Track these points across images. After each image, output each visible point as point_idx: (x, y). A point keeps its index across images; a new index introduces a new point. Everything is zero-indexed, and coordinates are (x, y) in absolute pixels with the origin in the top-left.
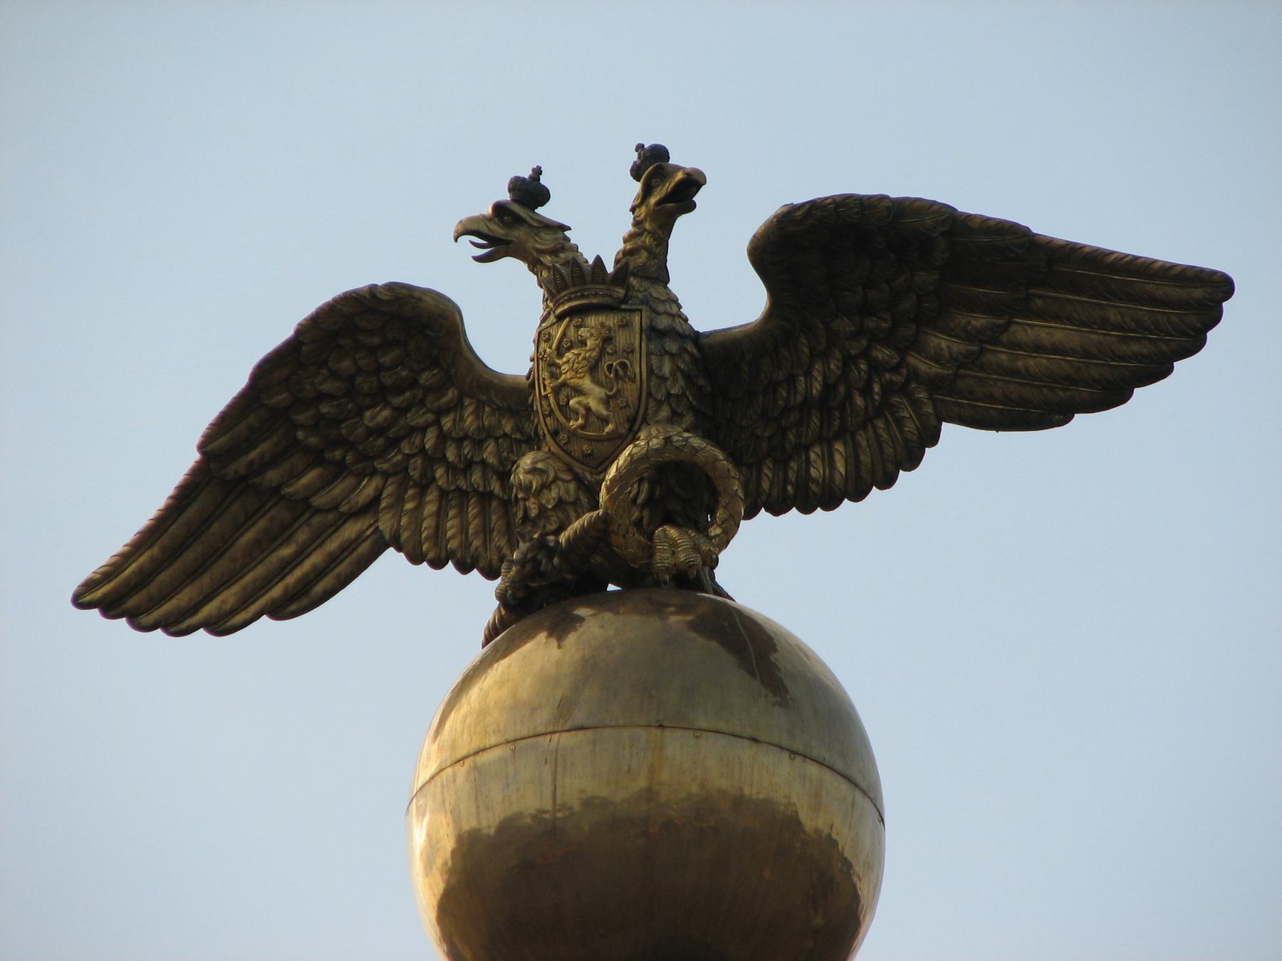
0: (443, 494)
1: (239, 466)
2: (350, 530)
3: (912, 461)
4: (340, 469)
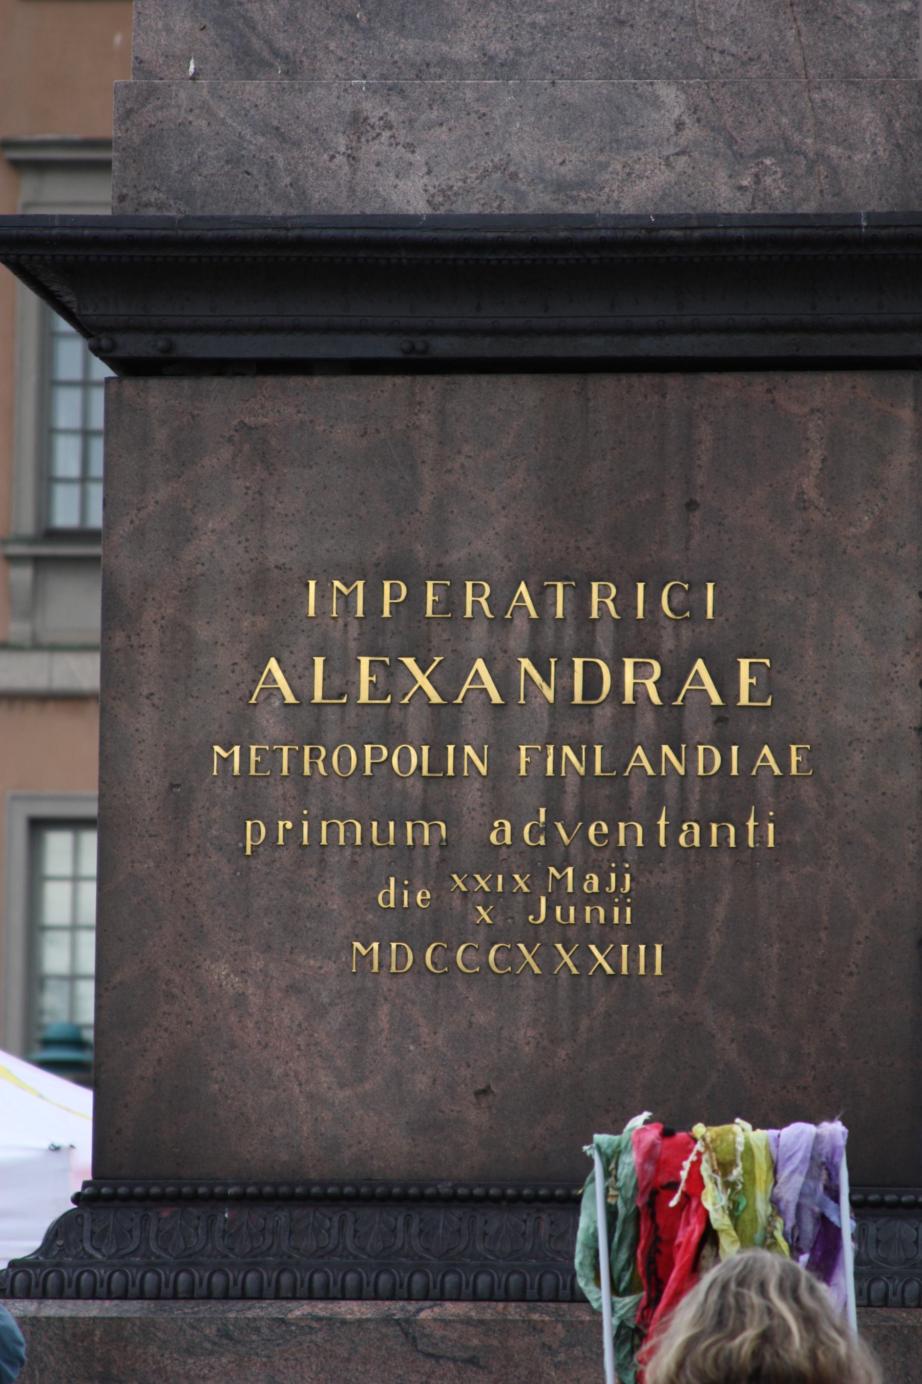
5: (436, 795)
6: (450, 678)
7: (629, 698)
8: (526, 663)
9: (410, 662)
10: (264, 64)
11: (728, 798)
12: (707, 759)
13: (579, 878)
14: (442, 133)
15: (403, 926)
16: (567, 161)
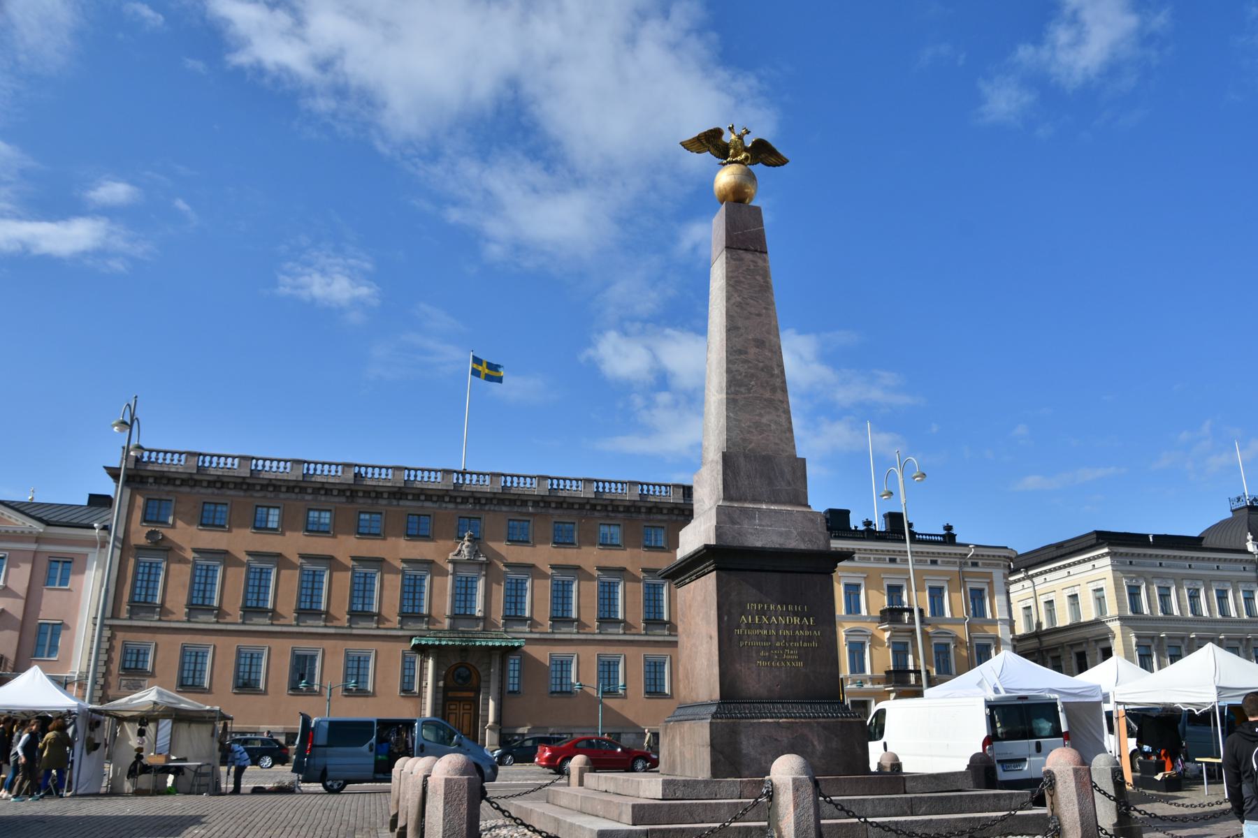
5: (769, 637)
6: (769, 619)
11: (809, 639)
12: (807, 633)
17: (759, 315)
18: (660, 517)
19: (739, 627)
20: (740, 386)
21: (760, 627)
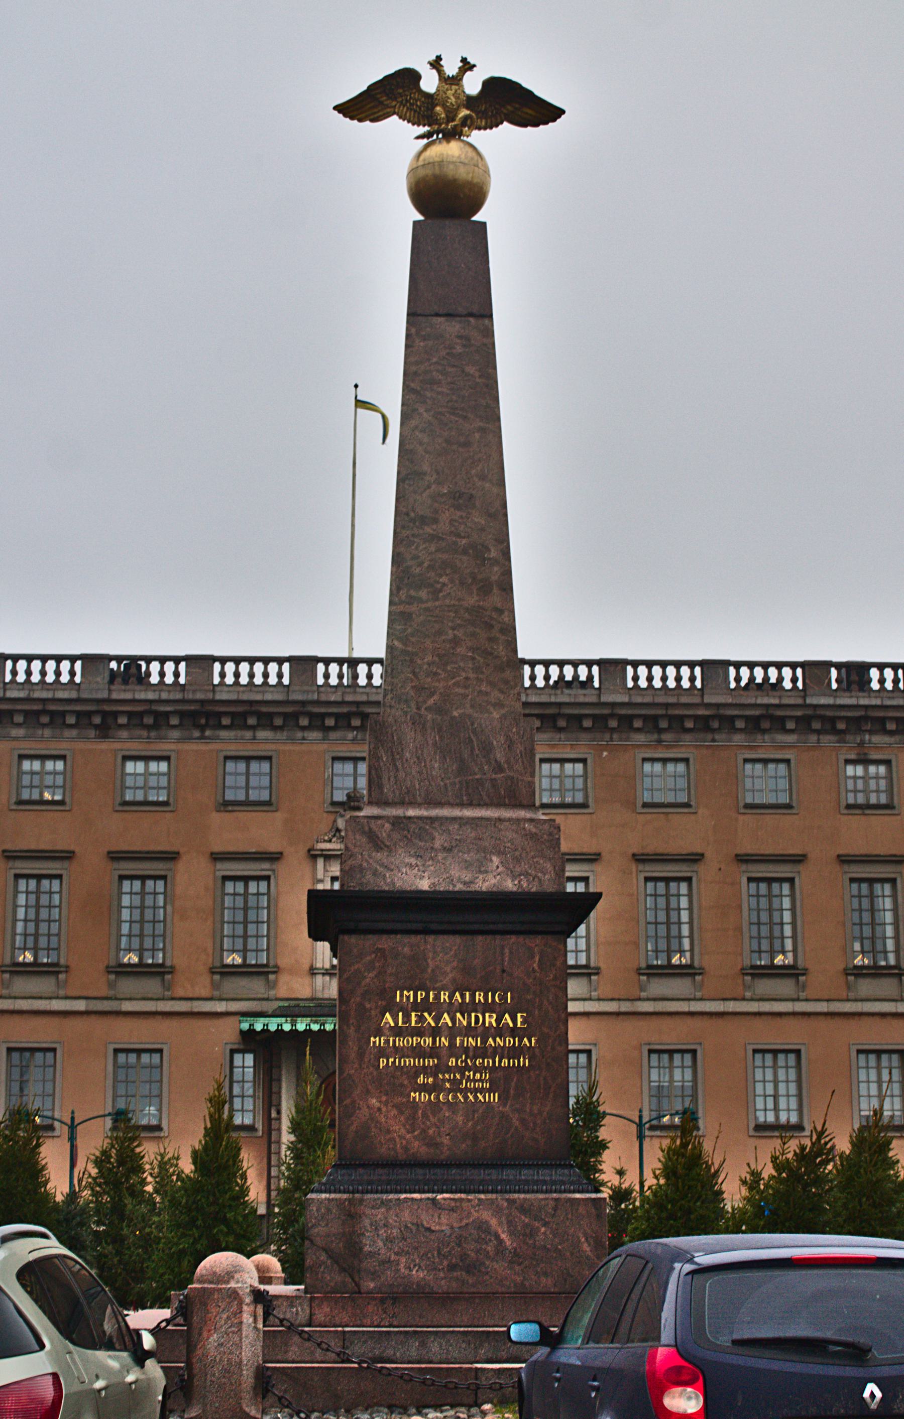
0: (408, 109)
1: (374, 93)
2: (388, 110)
3: (497, 126)
4: (390, 98)
5: (434, 1052)
6: (437, 1019)
7: (487, 1025)
8: (458, 1015)
9: (426, 1014)
10: (381, 849)
11: (513, 1052)
12: (509, 1041)
13: (474, 1075)
14: (432, 868)
15: (424, 1088)
16: (467, 876)
17: (467, 444)
18: (781, 738)
19: (379, 1032)
20: (418, 588)
21: (419, 1032)
